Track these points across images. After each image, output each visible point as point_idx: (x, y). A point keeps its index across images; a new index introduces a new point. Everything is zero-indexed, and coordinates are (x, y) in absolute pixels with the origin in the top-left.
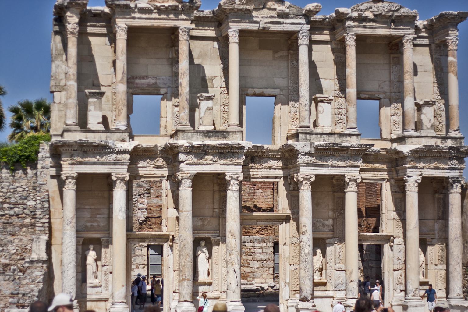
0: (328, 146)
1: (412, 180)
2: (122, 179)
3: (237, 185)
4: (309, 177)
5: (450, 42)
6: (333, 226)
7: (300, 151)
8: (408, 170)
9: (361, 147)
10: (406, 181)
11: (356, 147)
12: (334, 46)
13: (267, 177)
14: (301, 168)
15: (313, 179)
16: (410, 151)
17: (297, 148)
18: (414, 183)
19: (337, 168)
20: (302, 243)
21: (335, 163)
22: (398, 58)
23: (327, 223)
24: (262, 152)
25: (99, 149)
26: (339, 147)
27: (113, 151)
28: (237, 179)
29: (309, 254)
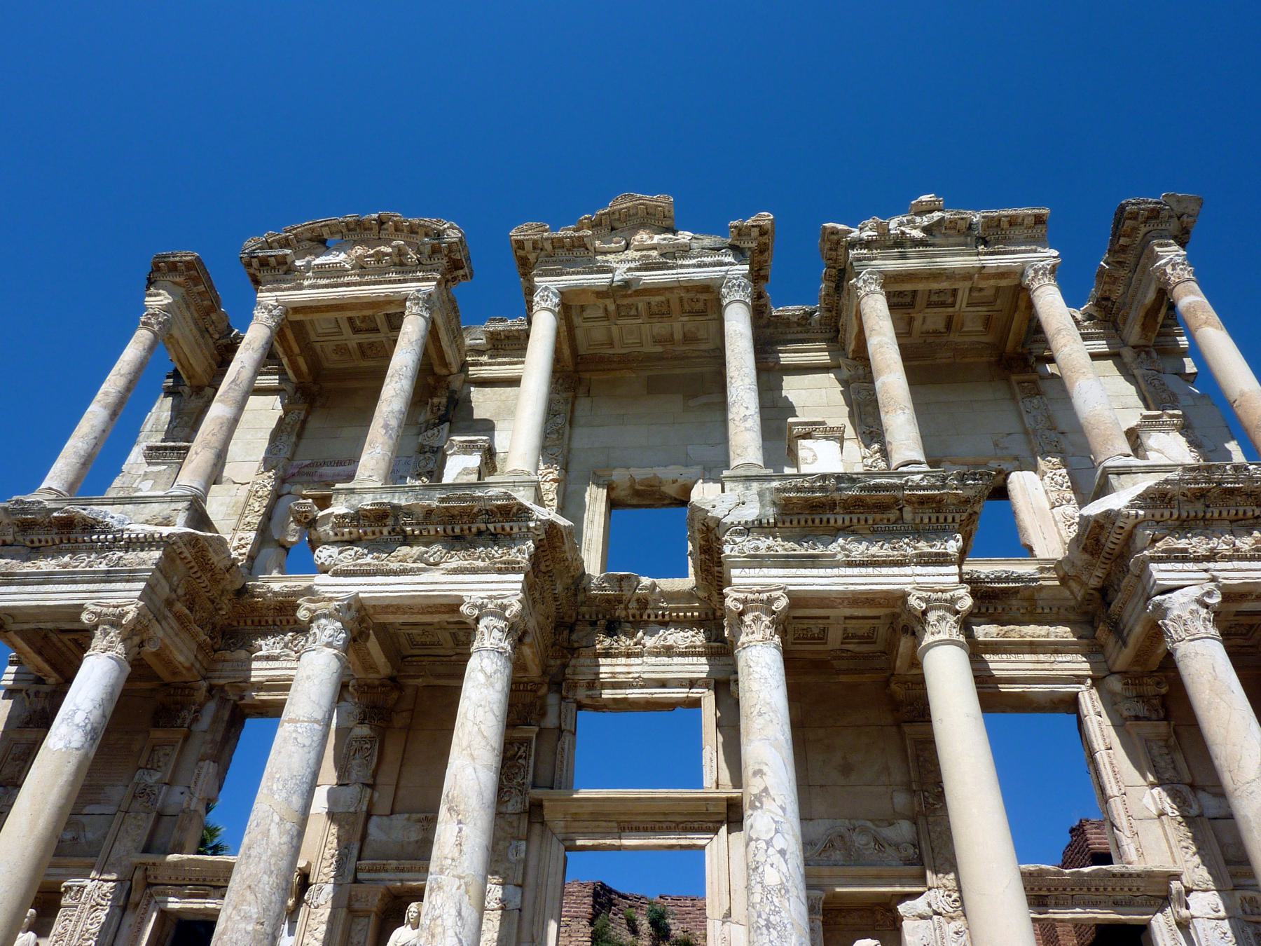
0: (822, 489)
1: (1185, 600)
2: (115, 622)
3: (496, 634)
4: (764, 596)
5: (1169, 270)
6: (916, 845)
7: (727, 520)
8: (1153, 566)
9: (943, 487)
10: (1161, 611)
11: (924, 488)
12: (846, 373)
13: (663, 684)
14: (734, 572)
15: (782, 603)
16: (1140, 497)
17: (717, 513)
18: (1195, 607)
19: (870, 570)
20: (753, 844)
21: (859, 549)
22: (1034, 382)
23: (888, 833)
24: (638, 600)
25: (73, 536)
26: (862, 489)
27: (115, 538)
28: (500, 612)
29: (783, 889)
